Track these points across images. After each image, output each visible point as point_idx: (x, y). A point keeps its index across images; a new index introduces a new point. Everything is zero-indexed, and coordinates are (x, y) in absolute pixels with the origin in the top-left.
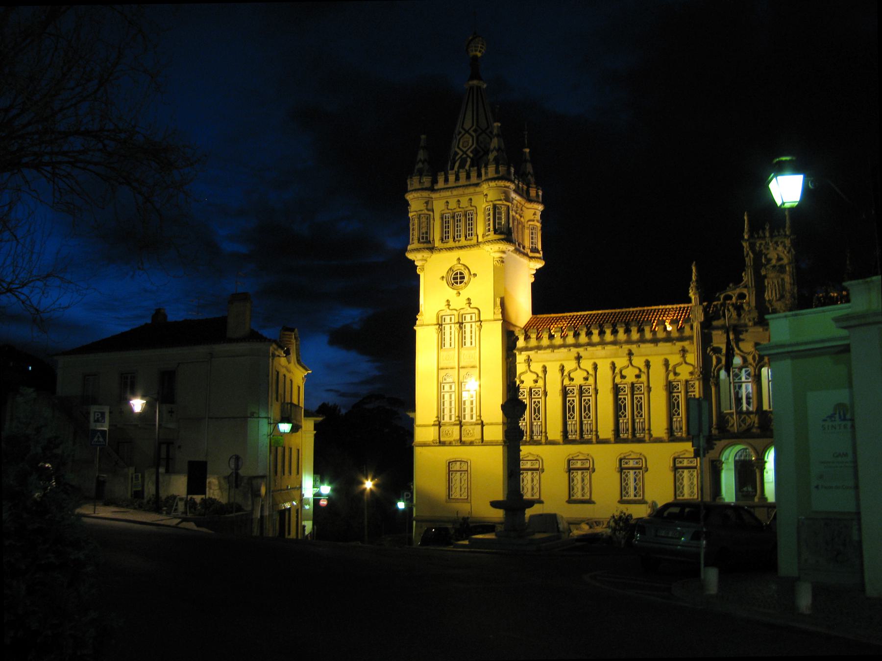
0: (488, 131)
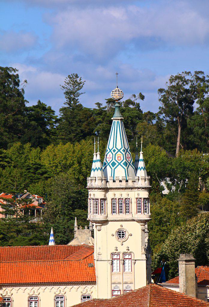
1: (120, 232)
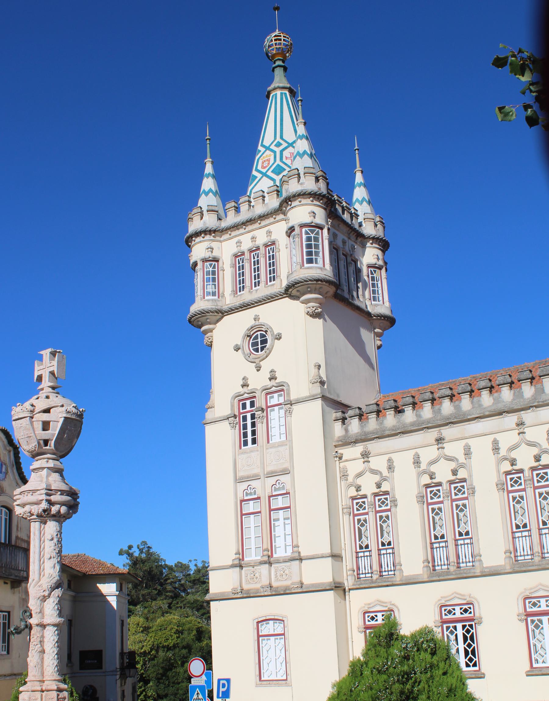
1: (256, 337)
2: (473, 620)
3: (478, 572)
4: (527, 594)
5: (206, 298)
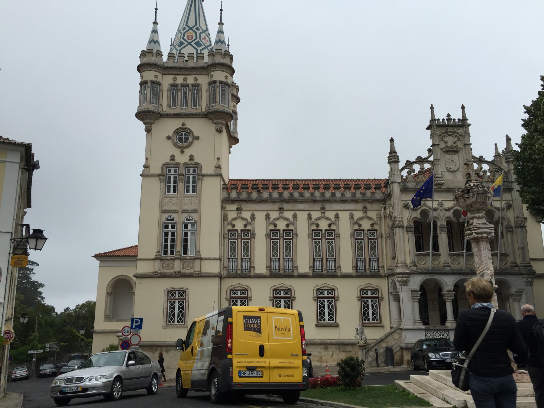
0: (207, 33)
1: (182, 135)
2: (290, 298)
3: (296, 274)
4: (319, 287)
5: (151, 104)
